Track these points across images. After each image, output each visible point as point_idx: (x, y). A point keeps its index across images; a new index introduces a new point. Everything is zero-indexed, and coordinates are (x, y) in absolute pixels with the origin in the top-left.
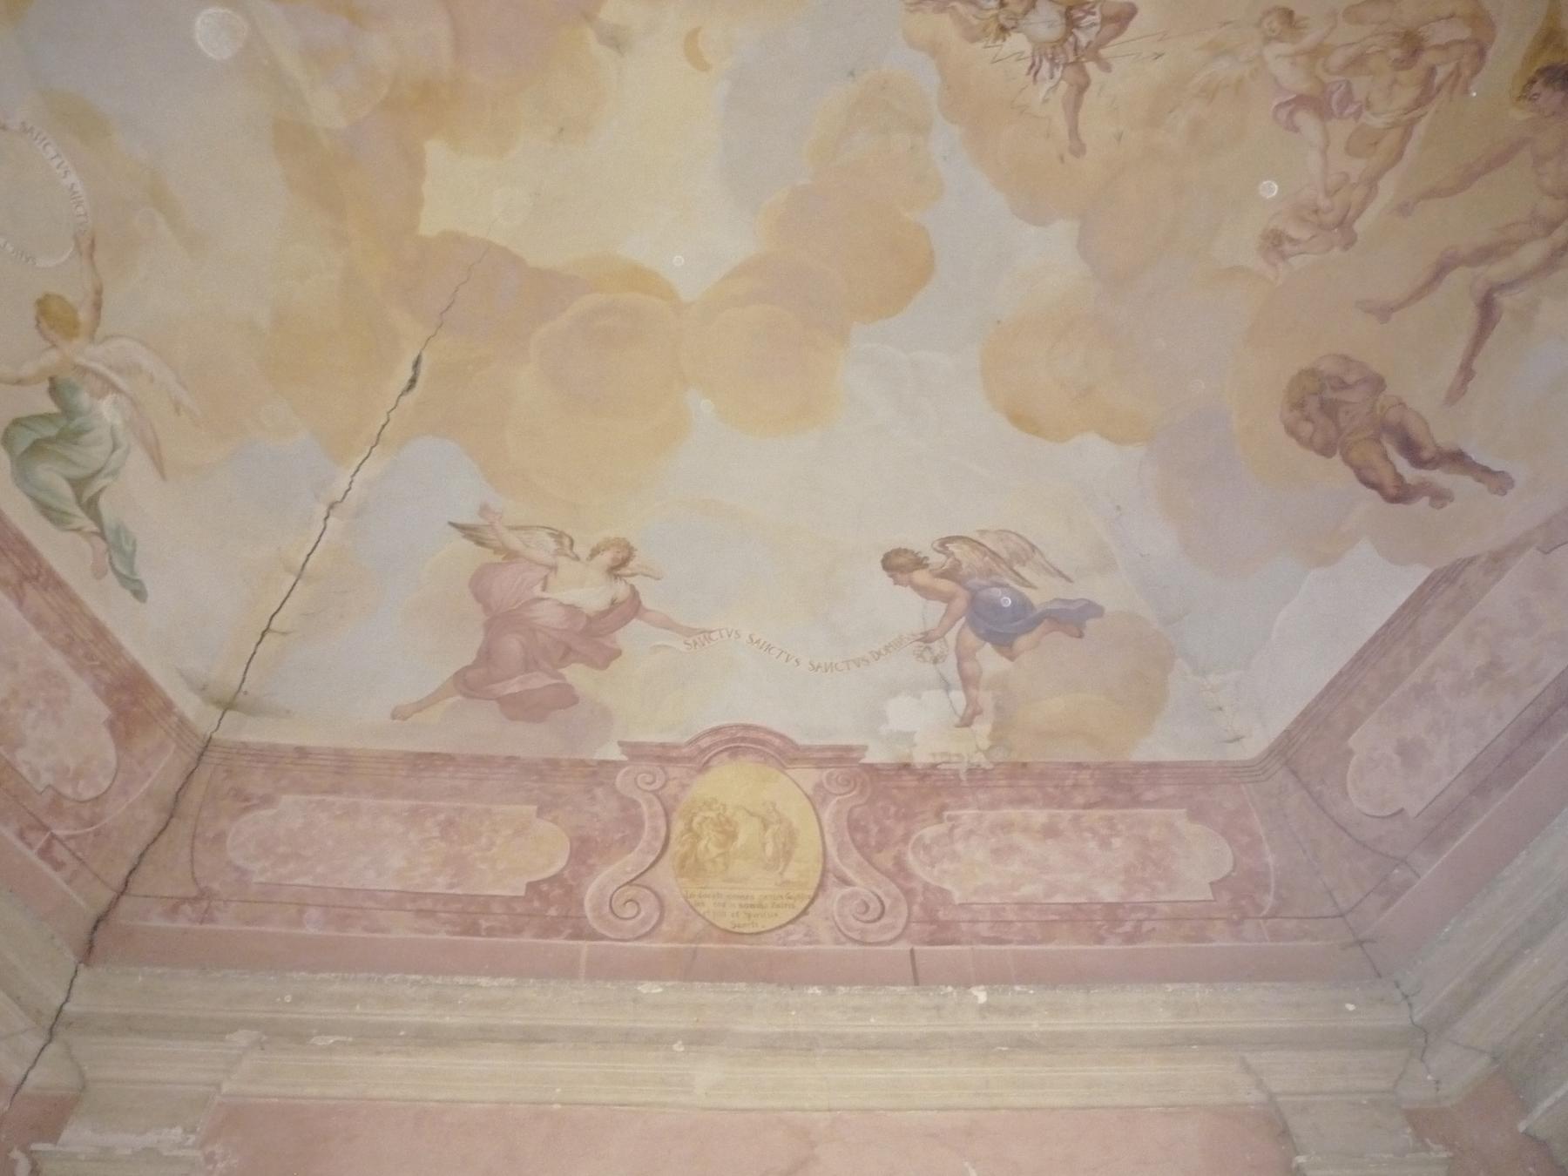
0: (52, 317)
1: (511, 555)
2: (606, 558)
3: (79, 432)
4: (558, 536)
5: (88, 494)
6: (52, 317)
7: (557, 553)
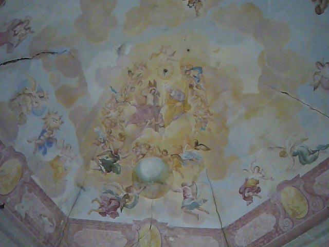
0: (283, 155)
1: (320, 82)
2: (320, 67)
3: (301, 152)
4: (315, 74)
5: (311, 152)
6: (283, 155)
7: (319, 74)
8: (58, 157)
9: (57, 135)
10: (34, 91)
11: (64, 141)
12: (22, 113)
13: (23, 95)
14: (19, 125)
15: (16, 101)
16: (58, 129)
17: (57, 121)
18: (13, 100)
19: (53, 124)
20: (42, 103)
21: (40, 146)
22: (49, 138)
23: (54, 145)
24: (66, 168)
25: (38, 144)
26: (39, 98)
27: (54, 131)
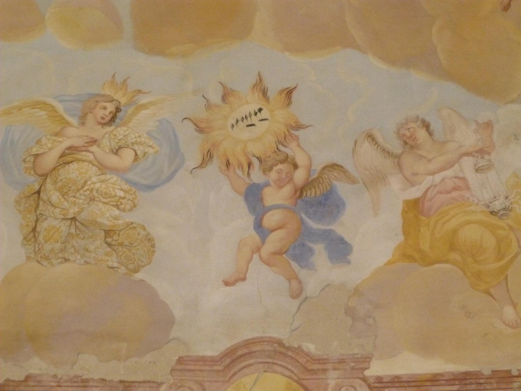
8: (415, 209)
9: (315, 151)
10: (71, 131)
11: (371, 137)
12: (108, 233)
13: (49, 185)
14: (138, 276)
15: (44, 225)
16: (299, 127)
17: (264, 114)
18: (34, 230)
19: (258, 139)
20: (140, 126)
21: (298, 251)
22: (300, 192)
23: (343, 189)
24: (497, 205)
25: (279, 253)
26: (108, 129)
27: (291, 150)
